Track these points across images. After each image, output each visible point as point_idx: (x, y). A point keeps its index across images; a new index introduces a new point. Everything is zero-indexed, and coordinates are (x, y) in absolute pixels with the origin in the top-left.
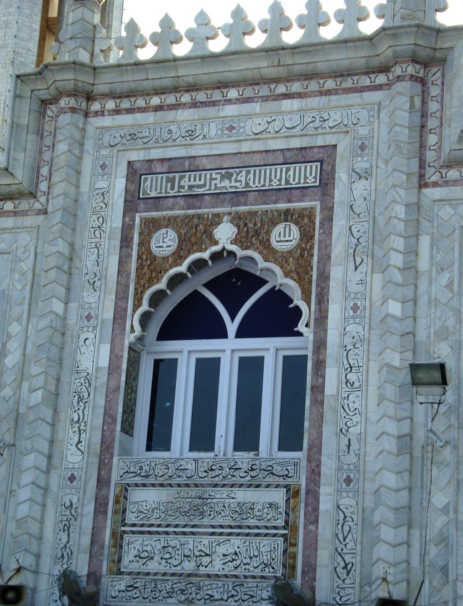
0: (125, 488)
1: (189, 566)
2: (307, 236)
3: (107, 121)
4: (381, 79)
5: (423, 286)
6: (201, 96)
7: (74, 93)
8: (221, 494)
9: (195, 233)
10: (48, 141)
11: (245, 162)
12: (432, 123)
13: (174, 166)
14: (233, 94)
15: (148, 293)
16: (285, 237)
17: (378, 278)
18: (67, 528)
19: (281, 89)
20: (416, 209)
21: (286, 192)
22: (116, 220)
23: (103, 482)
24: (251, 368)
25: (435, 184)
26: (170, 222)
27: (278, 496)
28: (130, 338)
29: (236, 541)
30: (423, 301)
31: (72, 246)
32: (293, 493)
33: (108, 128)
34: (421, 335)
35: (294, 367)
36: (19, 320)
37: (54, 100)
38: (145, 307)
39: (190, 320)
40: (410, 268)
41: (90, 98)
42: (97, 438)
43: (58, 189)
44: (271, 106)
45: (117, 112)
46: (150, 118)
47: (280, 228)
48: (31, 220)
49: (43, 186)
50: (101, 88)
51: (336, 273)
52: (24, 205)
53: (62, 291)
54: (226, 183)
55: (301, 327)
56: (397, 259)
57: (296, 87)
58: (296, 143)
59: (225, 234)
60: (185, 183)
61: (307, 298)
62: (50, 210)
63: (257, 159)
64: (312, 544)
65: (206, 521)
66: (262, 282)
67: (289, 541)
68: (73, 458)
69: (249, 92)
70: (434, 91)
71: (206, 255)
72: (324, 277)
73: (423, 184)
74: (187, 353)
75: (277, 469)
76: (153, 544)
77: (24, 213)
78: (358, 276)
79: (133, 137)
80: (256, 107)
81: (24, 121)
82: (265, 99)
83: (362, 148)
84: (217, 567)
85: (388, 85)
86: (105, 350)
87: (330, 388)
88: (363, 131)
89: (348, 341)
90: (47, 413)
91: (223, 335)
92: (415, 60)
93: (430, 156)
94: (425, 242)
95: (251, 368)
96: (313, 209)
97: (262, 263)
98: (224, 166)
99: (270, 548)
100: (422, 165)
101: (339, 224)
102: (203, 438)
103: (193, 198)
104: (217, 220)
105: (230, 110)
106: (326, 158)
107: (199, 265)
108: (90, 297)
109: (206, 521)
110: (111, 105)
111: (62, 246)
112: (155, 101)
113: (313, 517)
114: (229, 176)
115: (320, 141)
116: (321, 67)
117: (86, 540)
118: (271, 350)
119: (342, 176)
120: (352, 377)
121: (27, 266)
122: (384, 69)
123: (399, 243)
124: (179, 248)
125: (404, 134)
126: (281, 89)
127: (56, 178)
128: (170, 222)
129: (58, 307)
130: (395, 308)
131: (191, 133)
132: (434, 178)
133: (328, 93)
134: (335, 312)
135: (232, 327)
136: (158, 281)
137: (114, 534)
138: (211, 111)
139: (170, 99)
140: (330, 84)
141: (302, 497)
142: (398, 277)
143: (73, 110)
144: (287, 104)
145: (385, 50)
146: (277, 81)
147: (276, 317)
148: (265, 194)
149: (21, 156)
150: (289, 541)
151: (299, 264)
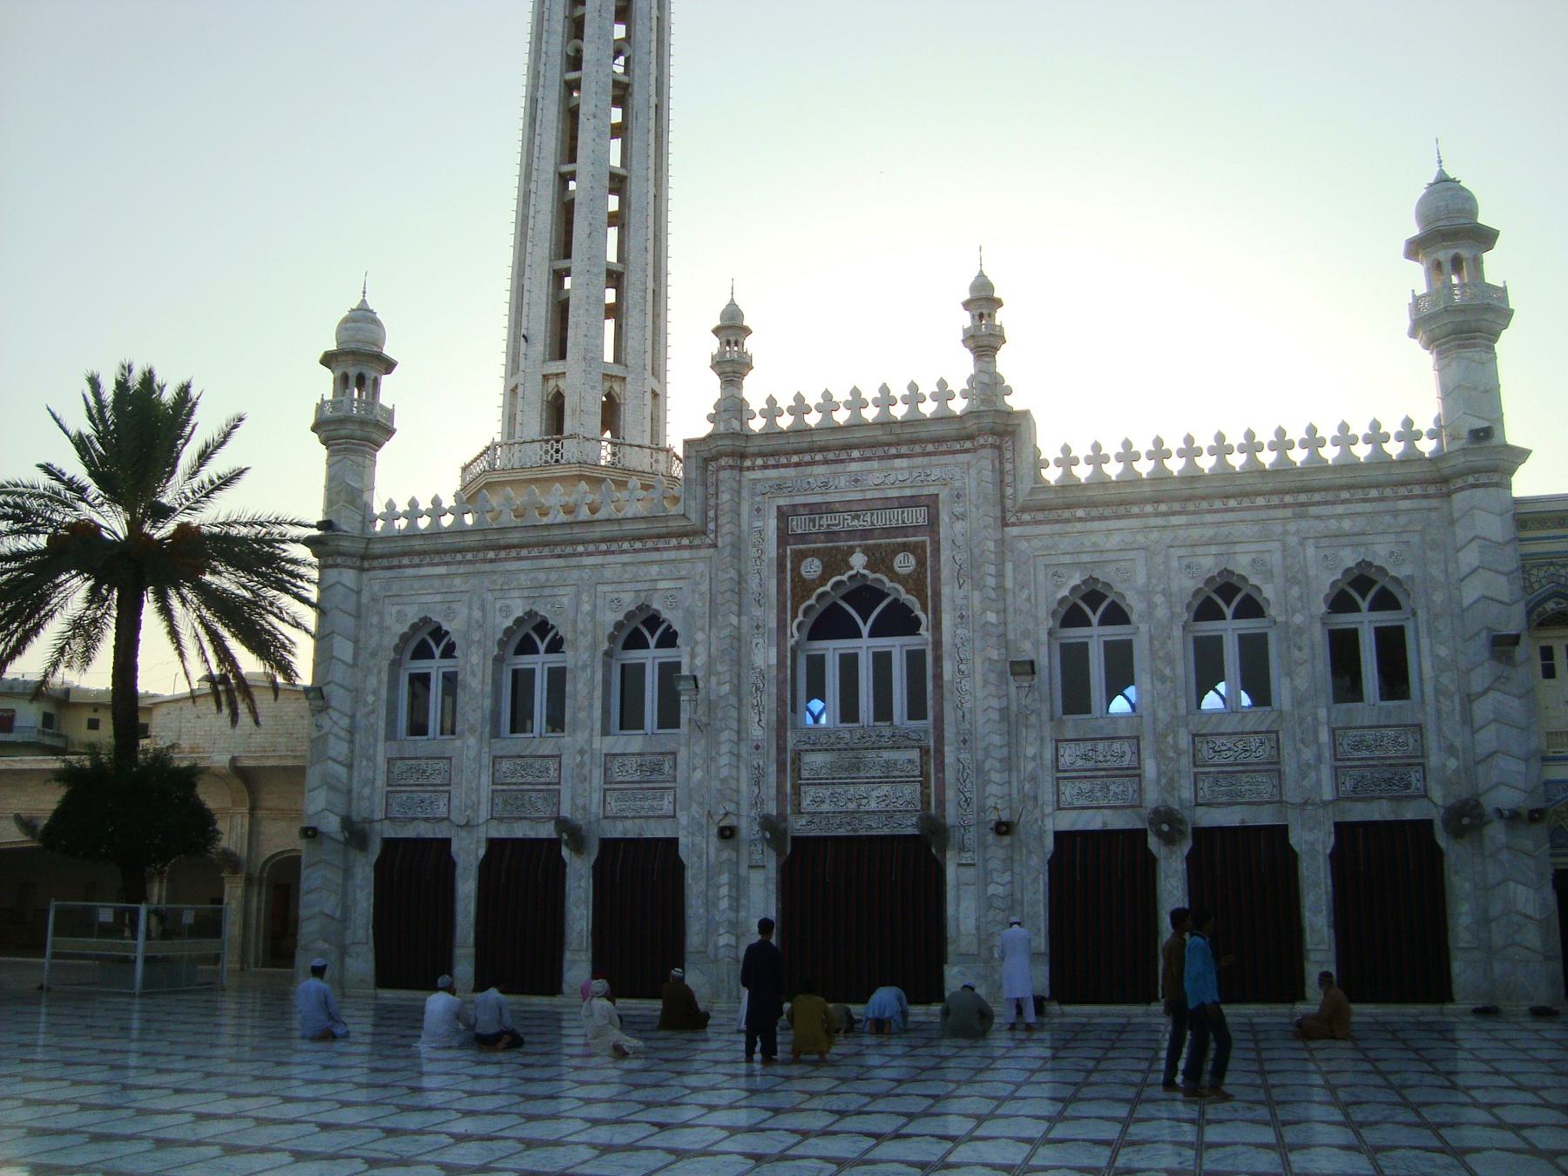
0: (798, 755)
1: (852, 806)
2: (921, 563)
3: (758, 474)
4: (968, 445)
5: (1010, 600)
6: (831, 456)
7: (731, 454)
8: (872, 755)
9: (835, 562)
10: (712, 490)
11: (869, 506)
12: (1008, 479)
13: (814, 510)
14: (855, 454)
15: (803, 607)
16: (904, 563)
17: (977, 594)
18: (757, 783)
19: (893, 451)
20: (1001, 542)
21: (903, 530)
22: (772, 551)
23: (781, 749)
24: (882, 662)
25: (1014, 525)
26: (815, 553)
27: (915, 755)
28: (791, 642)
29: (885, 789)
30: (1011, 609)
31: (739, 572)
32: (925, 752)
33: (759, 480)
34: (1011, 636)
35: (915, 660)
36: (702, 629)
37: (715, 458)
38: (800, 618)
39: (831, 624)
40: (1000, 587)
41: (743, 456)
42: (774, 717)
43: (725, 530)
44: (887, 463)
45: (765, 467)
46: (791, 472)
47: (900, 557)
48: (703, 553)
49: (711, 526)
50: (752, 450)
51: (946, 591)
52: (697, 541)
53: (735, 608)
54: (856, 522)
55: (922, 631)
56: (991, 582)
57: (904, 449)
58: (908, 492)
59: (858, 561)
60: (824, 522)
61: (925, 610)
62: (720, 544)
63: (879, 504)
64: (941, 785)
65: (862, 774)
66: (884, 595)
67: (925, 785)
68: (757, 732)
69: (868, 453)
70: (1008, 455)
71: (844, 578)
72: (937, 594)
73: (1005, 524)
74: (832, 650)
75: (913, 736)
76: (824, 792)
77: (698, 547)
78: (961, 593)
79: (780, 487)
80: (875, 464)
81: (693, 476)
82: (881, 458)
83: (958, 496)
84: (873, 805)
85: (975, 450)
86: (773, 652)
87: (947, 676)
88: (958, 484)
89: (958, 641)
90: (733, 700)
91: (857, 634)
92: (993, 433)
93: (1009, 503)
94: (1009, 567)
95: (882, 662)
96: (924, 542)
97: (888, 584)
98: (850, 508)
99: (911, 791)
100: (1003, 510)
101: (945, 554)
103: (831, 535)
104: (851, 551)
105: (854, 466)
106: (931, 504)
107: (838, 584)
108: (757, 612)
109: (862, 774)
110: (759, 462)
111: (733, 574)
112: (795, 459)
113: (941, 767)
114: (857, 517)
115: (926, 491)
116: (923, 435)
117: (773, 792)
118: (897, 646)
119: (944, 518)
120: (963, 667)
121: (704, 587)
122: (971, 438)
123: (992, 569)
124: (823, 572)
125: (990, 489)
126: (893, 451)
127: (722, 520)
128: (815, 553)
129: (734, 620)
130: (992, 617)
131: (825, 484)
132: (1013, 520)
133: (929, 454)
134: (947, 621)
135: (865, 630)
136: (809, 598)
137: (793, 786)
138: (839, 467)
139: (807, 458)
140: (930, 448)
141: (932, 755)
142: (993, 595)
143: (732, 467)
144: (898, 463)
145: (971, 425)
146: (890, 445)
147: (899, 621)
148: (886, 532)
149: (693, 503)
150: (925, 785)
151: (916, 583)
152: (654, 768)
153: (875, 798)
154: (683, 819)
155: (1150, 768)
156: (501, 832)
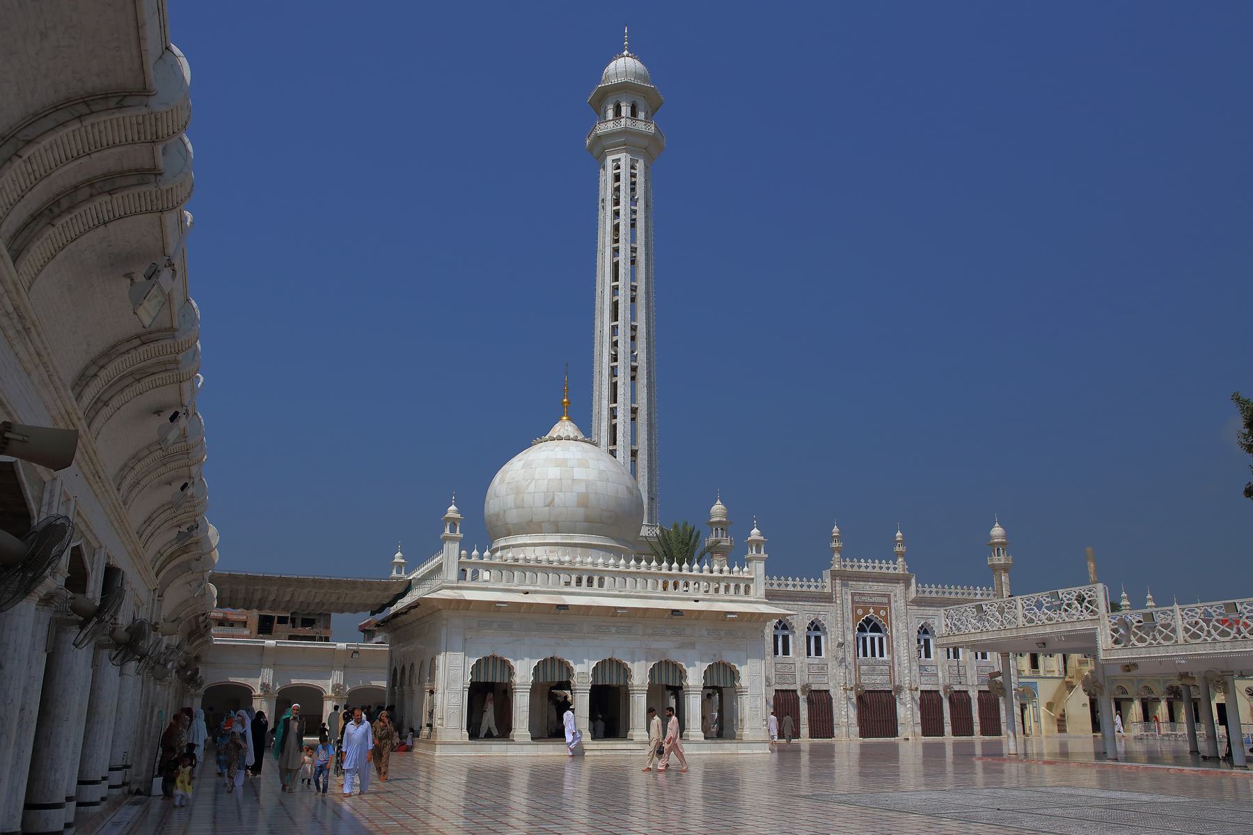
9: (866, 611)
24: (872, 639)
59: (871, 610)
95: (872, 639)
102: (873, 654)
141: (892, 668)
147: (876, 629)
151: (885, 618)
152: (822, 668)
153: (879, 679)
155: (940, 674)
156: (779, 688)
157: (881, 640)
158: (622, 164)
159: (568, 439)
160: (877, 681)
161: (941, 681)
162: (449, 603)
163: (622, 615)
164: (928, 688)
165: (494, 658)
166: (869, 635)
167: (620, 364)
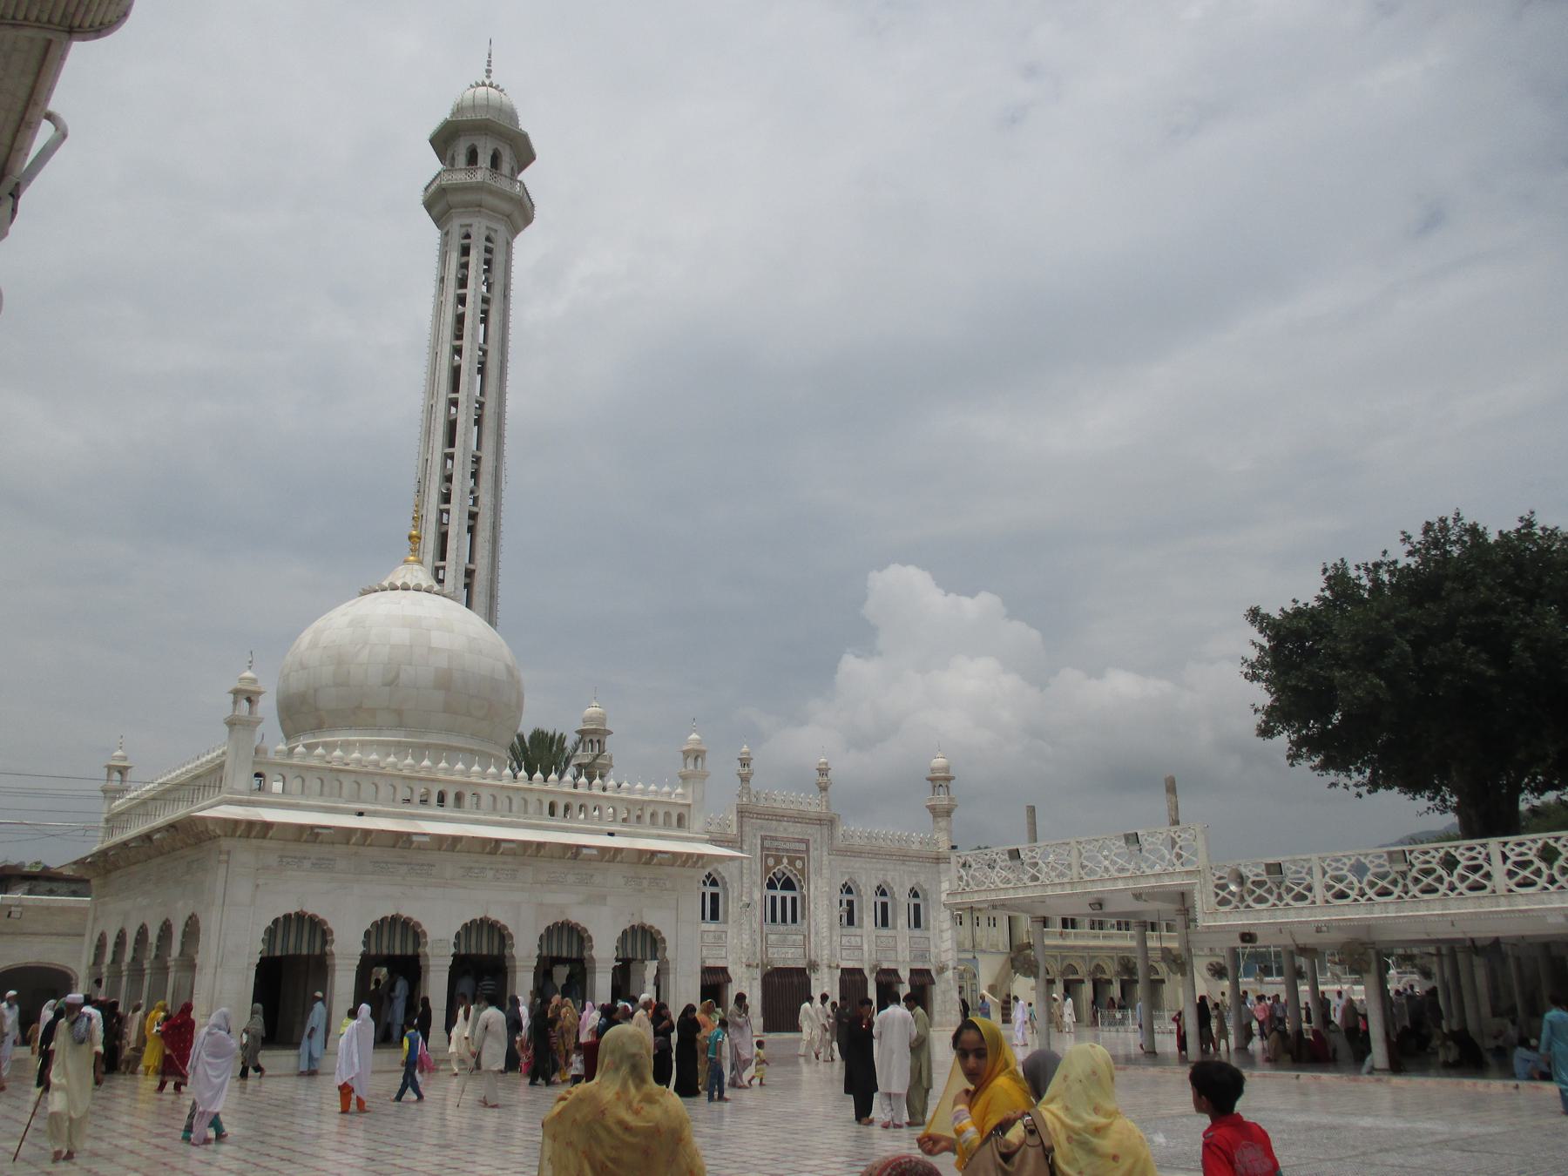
11: (788, 840)
24: (784, 899)
35: (794, 900)
59: (785, 861)
95: (784, 899)
106: (807, 842)
118: (789, 894)
141: (806, 938)
151: (802, 872)
152: (720, 938)
154: (730, 958)
155: (866, 947)
157: (794, 900)
158: (473, 232)
159: (418, 589)
160: (787, 956)
161: (866, 955)
162: (232, 826)
163: (513, 853)
164: (850, 965)
165: (300, 917)
166: (779, 893)
167: (454, 506)
